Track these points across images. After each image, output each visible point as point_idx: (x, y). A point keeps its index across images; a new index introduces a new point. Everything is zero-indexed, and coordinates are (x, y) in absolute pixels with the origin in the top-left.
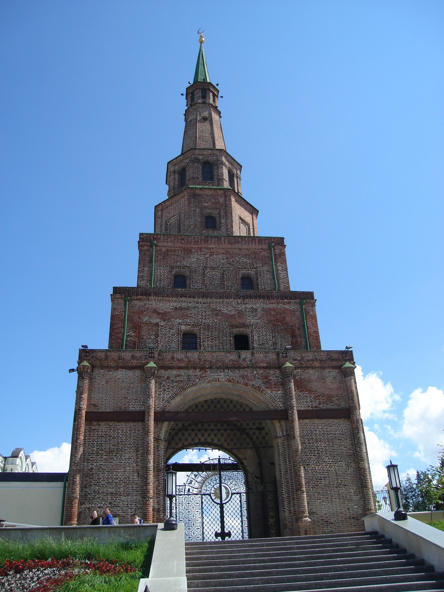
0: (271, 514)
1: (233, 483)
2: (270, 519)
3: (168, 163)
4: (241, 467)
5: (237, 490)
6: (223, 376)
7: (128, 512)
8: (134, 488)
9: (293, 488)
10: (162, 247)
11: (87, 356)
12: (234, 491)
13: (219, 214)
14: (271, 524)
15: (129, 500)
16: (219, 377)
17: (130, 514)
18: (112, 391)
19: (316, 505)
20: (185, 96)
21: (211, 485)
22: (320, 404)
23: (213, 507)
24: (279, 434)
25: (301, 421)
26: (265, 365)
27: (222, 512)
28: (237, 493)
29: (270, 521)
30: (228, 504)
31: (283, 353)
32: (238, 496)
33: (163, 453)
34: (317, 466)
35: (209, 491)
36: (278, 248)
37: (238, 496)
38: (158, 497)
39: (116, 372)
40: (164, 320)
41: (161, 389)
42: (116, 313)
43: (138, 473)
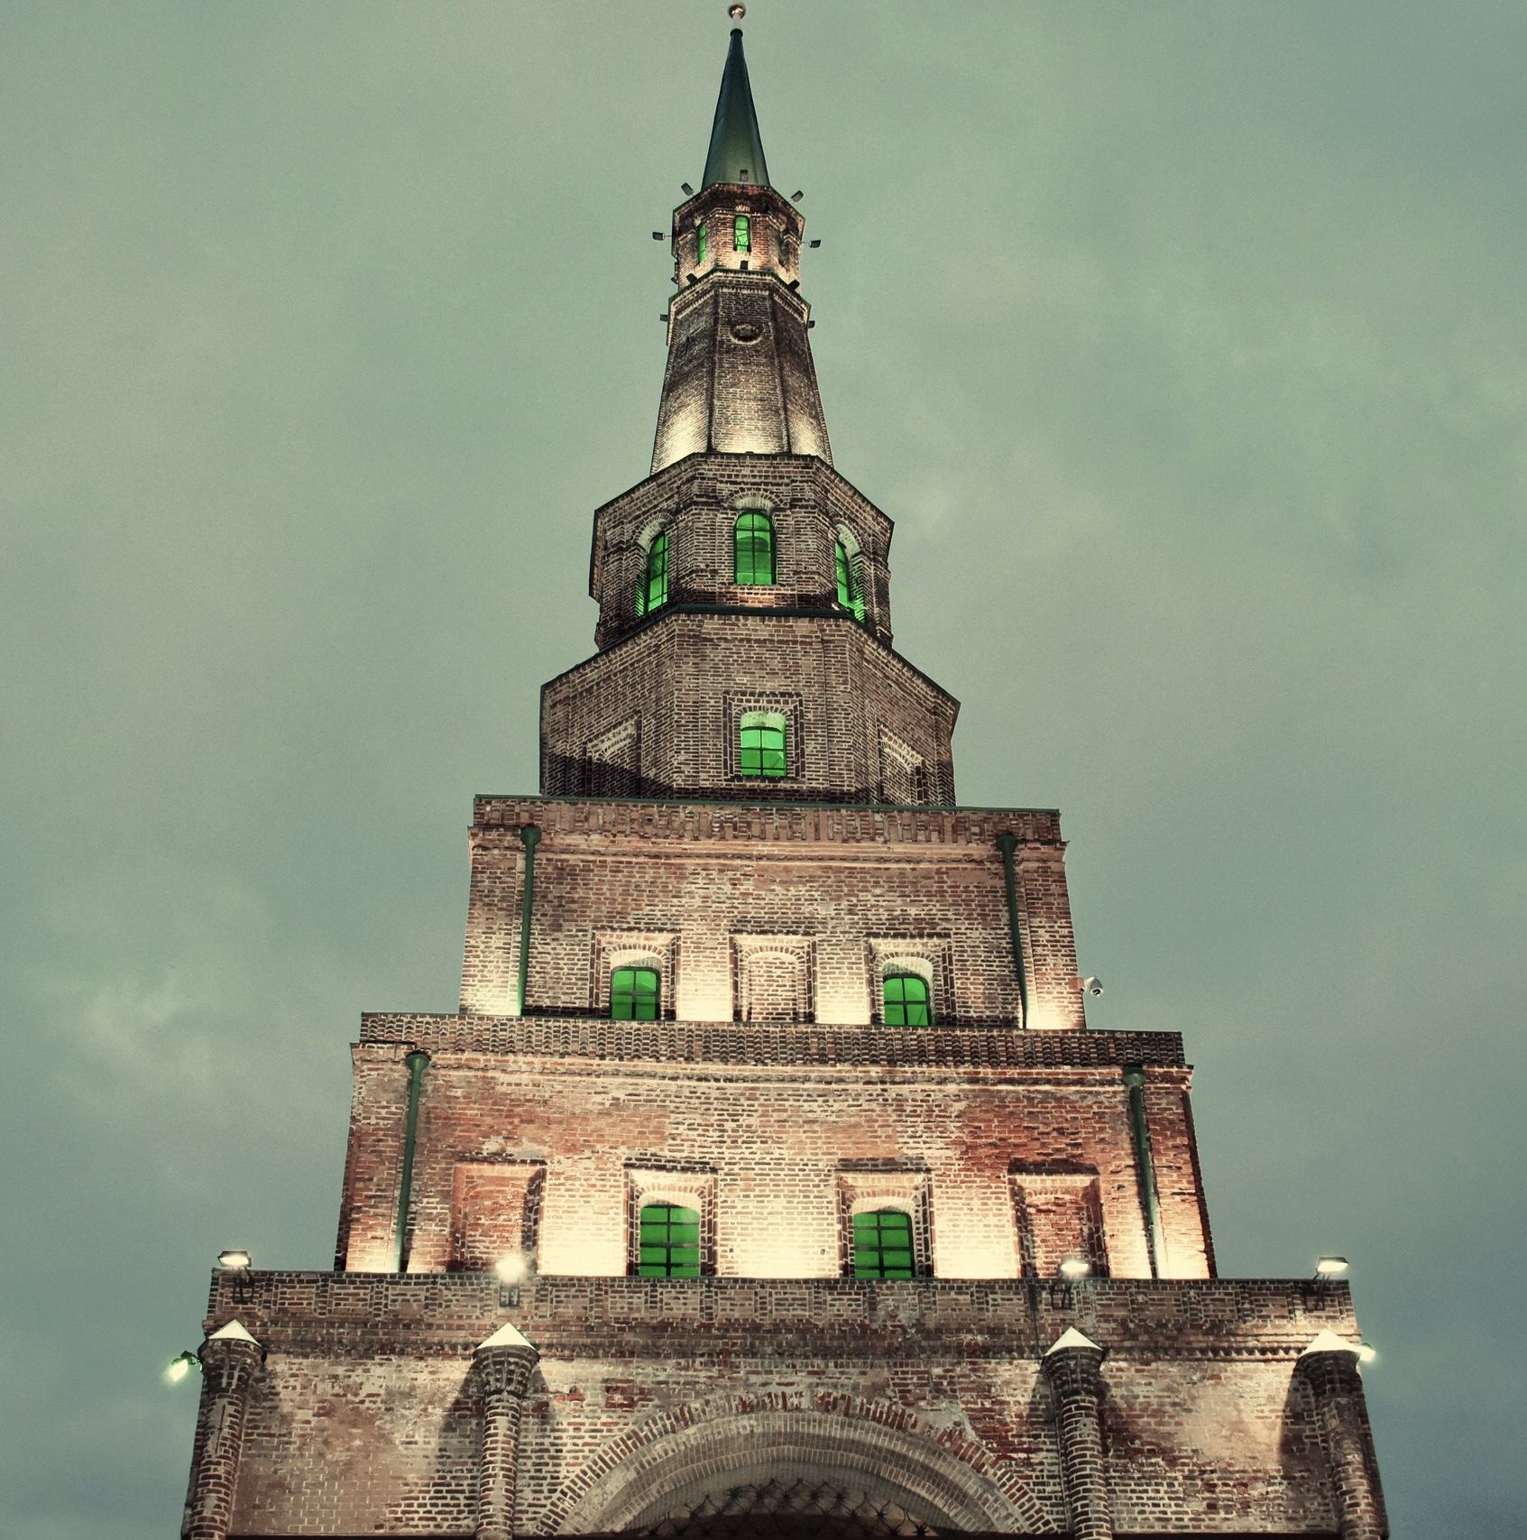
3: (599, 512)
6: (801, 1388)
11: (243, 1301)
16: (789, 1390)
20: (668, 240)
22: (1212, 1507)
26: (979, 1338)
31: (1052, 1291)
36: (1036, 854)
41: (547, 1441)
42: (373, 1121)
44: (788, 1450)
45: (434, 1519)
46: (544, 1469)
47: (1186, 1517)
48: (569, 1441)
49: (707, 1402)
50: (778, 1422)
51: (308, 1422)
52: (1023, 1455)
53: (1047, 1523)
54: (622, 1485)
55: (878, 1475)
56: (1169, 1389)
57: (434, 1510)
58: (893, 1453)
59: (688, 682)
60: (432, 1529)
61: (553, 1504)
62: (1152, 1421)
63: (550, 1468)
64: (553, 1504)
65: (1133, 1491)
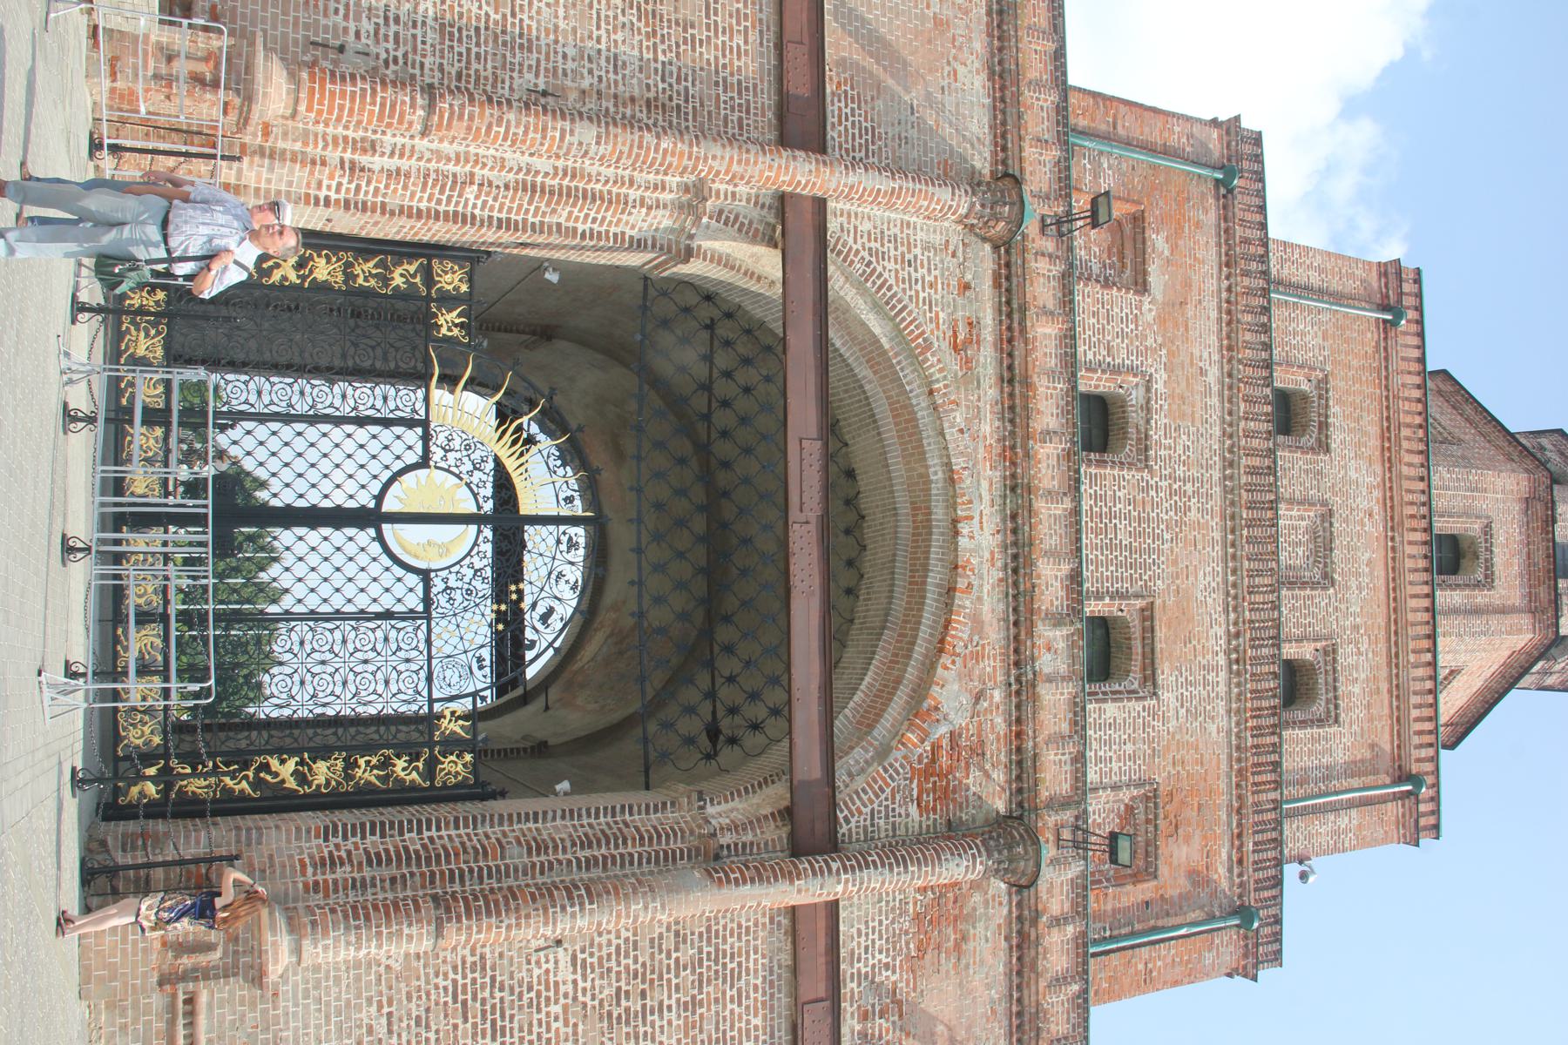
0: (321, 767)
1: (477, 583)
2: (291, 765)
5: (443, 599)
7: (358, 19)
8: (474, 66)
9: (452, 880)
10: (1386, 349)
12: (438, 585)
13: (1477, 585)
14: (266, 767)
15: (419, 32)
17: (352, 26)
18: (904, 36)
19: (359, 1008)
21: (470, 473)
23: (363, 477)
24: (720, 812)
25: (785, 922)
26: (1031, 744)
27: (338, 518)
28: (427, 600)
29: (283, 762)
30: (376, 548)
32: (414, 602)
34: (565, 1008)
35: (444, 458)
37: (414, 602)
38: (427, 176)
39: (977, 65)
40: (1161, 320)
41: (918, 251)
43: (545, 94)
44: (905, 528)
45: (840, 123)
46: (892, 246)
47: (854, 985)
48: (919, 276)
49: (961, 431)
50: (939, 513)
51: (928, 7)
52: (915, 793)
53: (847, 821)
54: (877, 330)
55: (884, 628)
56: (982, 961)
57: (849, 124)
58: (913, 643)
59: (1499, 483)
60: (830, 120)
61: (857, 252)
62: (951, 944)
63: (893, 253)
64: (857, 252)
65: (880, 922)
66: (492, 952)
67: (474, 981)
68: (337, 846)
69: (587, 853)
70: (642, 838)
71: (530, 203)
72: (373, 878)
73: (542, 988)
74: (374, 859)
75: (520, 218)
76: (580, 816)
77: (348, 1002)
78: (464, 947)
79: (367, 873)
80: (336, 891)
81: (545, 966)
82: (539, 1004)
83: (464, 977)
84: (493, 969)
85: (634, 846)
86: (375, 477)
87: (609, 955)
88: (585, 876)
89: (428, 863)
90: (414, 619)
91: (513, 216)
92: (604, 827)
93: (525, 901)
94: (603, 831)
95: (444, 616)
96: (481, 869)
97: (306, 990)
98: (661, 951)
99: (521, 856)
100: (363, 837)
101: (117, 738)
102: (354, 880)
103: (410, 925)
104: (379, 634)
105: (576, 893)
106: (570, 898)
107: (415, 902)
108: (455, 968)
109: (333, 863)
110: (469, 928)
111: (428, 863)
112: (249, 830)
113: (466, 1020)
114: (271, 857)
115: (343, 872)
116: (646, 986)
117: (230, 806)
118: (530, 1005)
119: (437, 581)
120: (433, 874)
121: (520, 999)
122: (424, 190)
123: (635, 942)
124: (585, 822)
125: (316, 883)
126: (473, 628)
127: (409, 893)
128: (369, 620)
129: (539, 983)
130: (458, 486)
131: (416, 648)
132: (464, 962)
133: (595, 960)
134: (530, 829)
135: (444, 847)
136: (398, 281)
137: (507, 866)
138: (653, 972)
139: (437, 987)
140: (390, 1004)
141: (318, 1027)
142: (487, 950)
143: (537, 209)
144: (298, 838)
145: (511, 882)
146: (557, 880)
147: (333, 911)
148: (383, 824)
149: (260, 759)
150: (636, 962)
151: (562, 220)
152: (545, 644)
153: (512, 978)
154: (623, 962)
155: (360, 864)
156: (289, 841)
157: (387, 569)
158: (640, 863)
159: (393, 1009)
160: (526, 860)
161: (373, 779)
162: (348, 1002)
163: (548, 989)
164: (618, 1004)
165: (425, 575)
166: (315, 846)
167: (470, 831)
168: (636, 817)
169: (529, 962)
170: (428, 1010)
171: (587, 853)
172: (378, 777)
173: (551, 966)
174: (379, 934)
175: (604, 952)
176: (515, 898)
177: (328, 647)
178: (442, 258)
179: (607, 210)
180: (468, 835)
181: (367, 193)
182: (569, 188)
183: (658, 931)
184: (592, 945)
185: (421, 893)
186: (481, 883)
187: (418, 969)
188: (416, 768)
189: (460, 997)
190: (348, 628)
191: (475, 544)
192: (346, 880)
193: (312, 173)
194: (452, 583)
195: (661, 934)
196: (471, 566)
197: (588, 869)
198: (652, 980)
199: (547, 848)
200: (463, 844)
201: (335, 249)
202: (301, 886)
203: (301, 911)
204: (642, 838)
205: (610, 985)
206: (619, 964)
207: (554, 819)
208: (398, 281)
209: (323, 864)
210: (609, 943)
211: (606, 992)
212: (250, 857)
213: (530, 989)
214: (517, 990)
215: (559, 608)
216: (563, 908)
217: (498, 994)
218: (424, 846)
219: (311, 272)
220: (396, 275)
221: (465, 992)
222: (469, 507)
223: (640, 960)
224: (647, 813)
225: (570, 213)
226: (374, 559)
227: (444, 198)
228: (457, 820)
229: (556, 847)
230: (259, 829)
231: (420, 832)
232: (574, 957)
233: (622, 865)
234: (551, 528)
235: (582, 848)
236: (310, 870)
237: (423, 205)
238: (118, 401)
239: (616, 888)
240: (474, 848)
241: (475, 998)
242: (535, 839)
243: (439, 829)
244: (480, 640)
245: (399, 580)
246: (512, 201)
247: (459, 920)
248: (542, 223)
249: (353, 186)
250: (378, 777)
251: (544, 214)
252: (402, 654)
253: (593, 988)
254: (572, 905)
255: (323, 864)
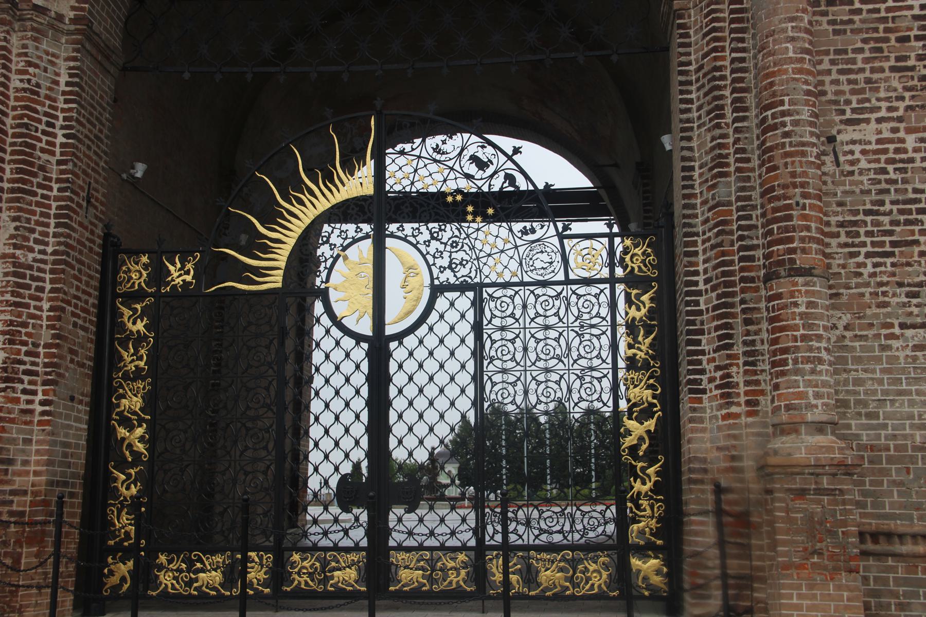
1: (446, 236)
4: (607, 202)
5: (463, 271)
9: (751, 259)
12: (447, 276)
14: (633, 449)
19: (893, 359)
27: (379, 379)
28: (462, 288)
29: (629, 433)
30: (410, 341)
32: (464, 302)
33: (63, 79)
34: (909, 131)
37: (464, 302)
66: (836, 214)
67: (869, 234)
68: (711, 380)
69: (728, 111)
70: (715, 49)
71: (35, 194)
72: (745, 343)
73: (883, 157)
74: (725, 343)
75: (54, 205)
76: (688, 121)
77: (883, 371)
78: (828, 245)
79: (739, 349)
80: (757, 383)
81: (857, 155)
82: (902, 161)
83: (864, 244)
84: (857, 213)
85: (723, 58)
86: (338, 343)
87: (850, 82)
88: (753, 112)
89: (732, 284)
90: (482, 300)
91: (53, 211)
92: (701, 93)
93: (776, 178)
94: (706, 95)
95: (479, 270)
96: (740, 228)
97: (869, 416)
98: (851, 21)
99: (728, 184)
100: (703, 353)
101: (601, 596)
102: (746, 363)
103: (796, 305)
104: (497, 336)
105: (770, 121)
106: (774, 127)
107: (770, 299)
108: (853, 255)
109: (728, 385)
110: (802, 239)
111: (732, 284)
112: (691, 471)
113: (917, 242)
114: (719, 449)
115: (739, 379)
116: (893, 37)
117: (670, 488)
118: (904, 171)
119: (443, 278)
120: (743, 279)
121: (895, 182)
122: (27, 306)
123: (837, 52)
124: (696, 115)
125: (748, 403)
126: (491, 239)
127: (763, 305)
128: (482, 347)
129: (878, 161)
130: (346, 258)
131: (512, 298)
132: (846, 245)
133: (854, 99)
134: (701, 175)
135: (715, 267)
136: (140, 326)
137: (738, 199)
138: (876, 30)
139: (873, 275)
140: (891, 326)
141: (912, 403)
142: (833, 220)
143: (40, 186)
144: (701, 420)
145: (755, 194)
146: (756, 143)
147: (776, 387)
148: (689, 332)
149: (626, 457)
150: (861, 50)
151: (53, 160)
152: (509, 165)
153: (869, 192)
154: (860, 65)
155: (729, 357)
156: (704, 430)
157: (431, 329)
158: (744, 50)
159: (896, 323)
160: (733, 178)
161: (648, 341)
162: (883, 371)
163: (886, 151)
164: (912, 69)
165: (437, 290)
166: (710, 404)
167: (700, 240)
168: (693, 57)
169: (852, 173)
170: (900, 285)
171: (728, 111)
172: (647, 335)
173: (857, 148)
174: (804, 338)
175: (846, 88)
176: (772, 189)
177: (510, 388)
178: (115, 283)
179: (37, 112)
180: (704, 242)
181: (33, 364)
182: (13, 153)
183: (825, 26)
184: (836, 102)
185: (763, 293)
186: (756, 227)
187: (850, 295)
188: (638, 296)
189: (888, 248)
190: (491, 367)
191: (404, 239)
192: (746, 372)
193: (12, 421)
194: (445, 262)
195: (830, 23)
196: (427, 243)
197: (746, 109)
198: (887, 30)
199: (720, 156)
200: (713, 247)
201: (112, 390)
202: (750, 420)
203: (776, 420)
204: (715, 49)
205: (887, 80)
206: (862, 70)
207: (690, 149)
208: (140, 326)
209: (728, 395)
210: (836, 82)
211: (895, 84)
212: (718, 470)
213: (884, 171)
214: (884, 186)
215: (471, 150)
216: (786, 135)
217: (888, 207)
218: (714, 289)
219: (135, 413)
220: (135, 329)
221: (882, 244)
222: (367, 246)
223: (859, 45)
224: (689, 45)
225: (43, 150)
226: (421, 342)
227: (34, 284)
228: (687, 254)
229: (721, 146)
230: (690, 460)
231: (699, 293)
232: (849, 122)
233: (744, 70)
234: (388, 161)
235: (722, 116)
236: (734, 409)
237: (46, 305)
238: (267, 597)
239: (768, 76)
240: (718, 235)
241: (890, 233)
242: (711, 169)
243: (696, 273)
244: (504, 232)
245: (442, 317)
246: (33, 213)
247: (793, 251)
248: (58, 181)
249: (26, 378)
250: (647, 335)
251: (46, 178)
252: (518, 313)
253: (888, 99)
254: (784, 124)
255: (728, 395)
